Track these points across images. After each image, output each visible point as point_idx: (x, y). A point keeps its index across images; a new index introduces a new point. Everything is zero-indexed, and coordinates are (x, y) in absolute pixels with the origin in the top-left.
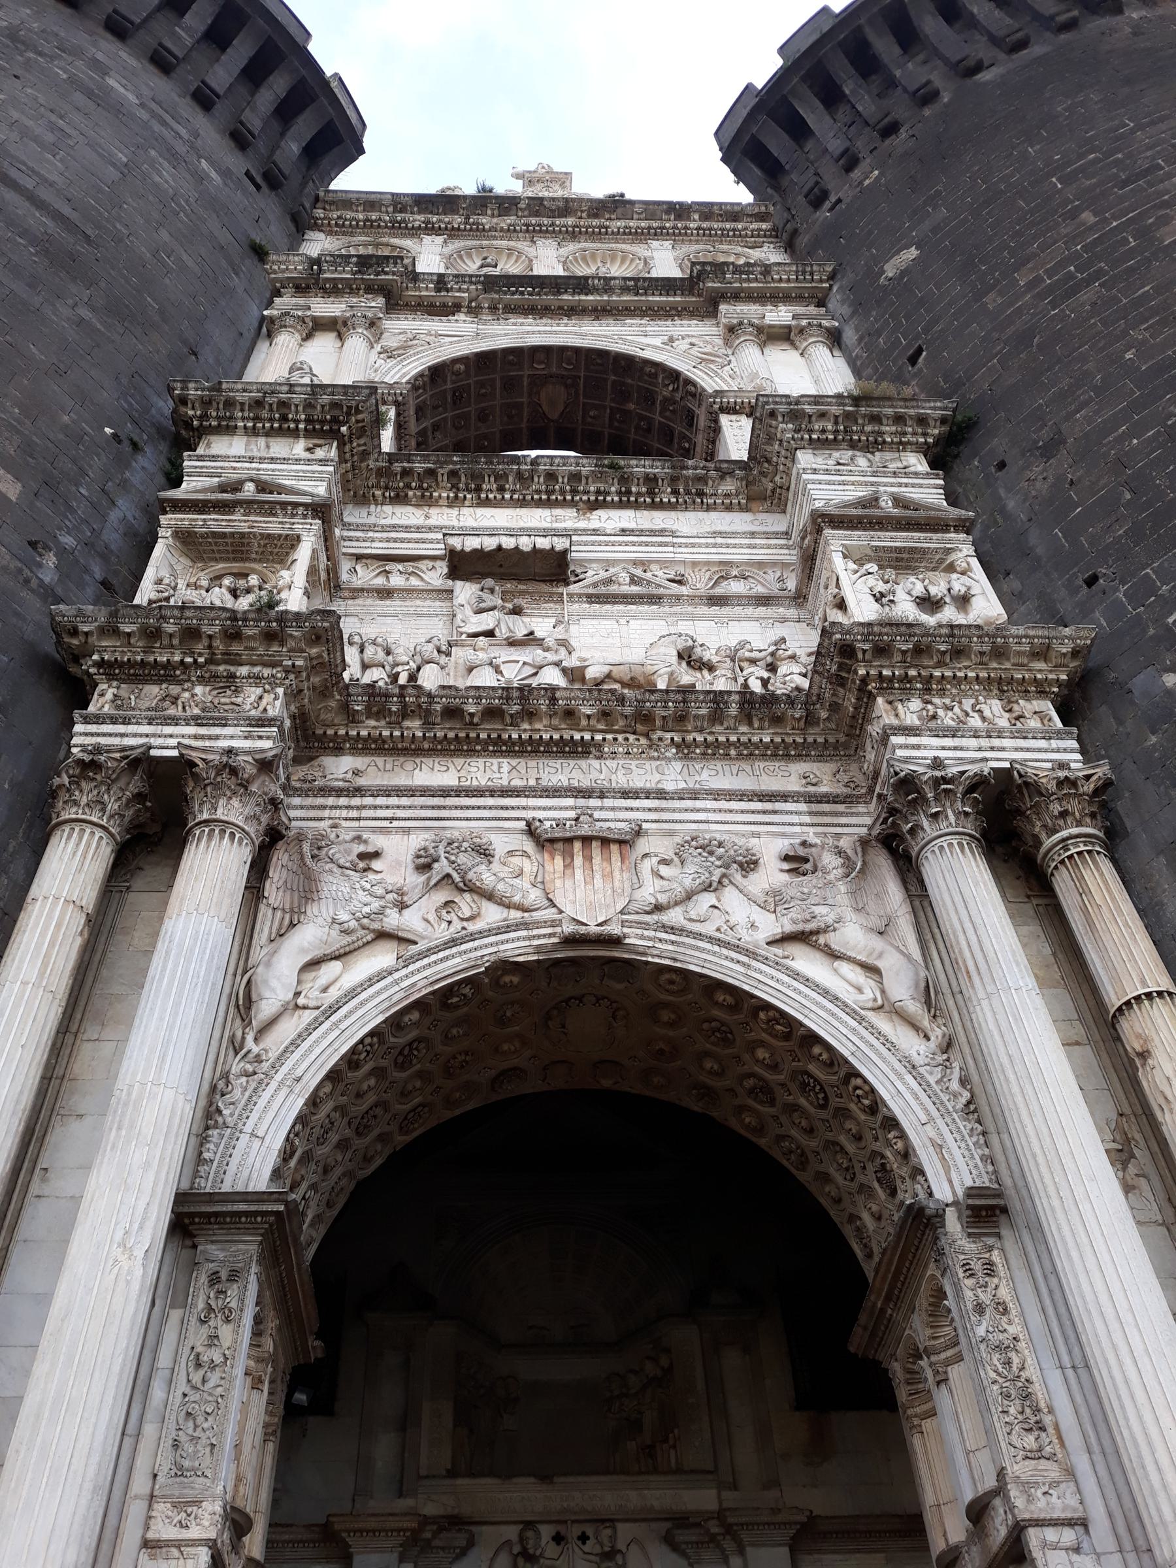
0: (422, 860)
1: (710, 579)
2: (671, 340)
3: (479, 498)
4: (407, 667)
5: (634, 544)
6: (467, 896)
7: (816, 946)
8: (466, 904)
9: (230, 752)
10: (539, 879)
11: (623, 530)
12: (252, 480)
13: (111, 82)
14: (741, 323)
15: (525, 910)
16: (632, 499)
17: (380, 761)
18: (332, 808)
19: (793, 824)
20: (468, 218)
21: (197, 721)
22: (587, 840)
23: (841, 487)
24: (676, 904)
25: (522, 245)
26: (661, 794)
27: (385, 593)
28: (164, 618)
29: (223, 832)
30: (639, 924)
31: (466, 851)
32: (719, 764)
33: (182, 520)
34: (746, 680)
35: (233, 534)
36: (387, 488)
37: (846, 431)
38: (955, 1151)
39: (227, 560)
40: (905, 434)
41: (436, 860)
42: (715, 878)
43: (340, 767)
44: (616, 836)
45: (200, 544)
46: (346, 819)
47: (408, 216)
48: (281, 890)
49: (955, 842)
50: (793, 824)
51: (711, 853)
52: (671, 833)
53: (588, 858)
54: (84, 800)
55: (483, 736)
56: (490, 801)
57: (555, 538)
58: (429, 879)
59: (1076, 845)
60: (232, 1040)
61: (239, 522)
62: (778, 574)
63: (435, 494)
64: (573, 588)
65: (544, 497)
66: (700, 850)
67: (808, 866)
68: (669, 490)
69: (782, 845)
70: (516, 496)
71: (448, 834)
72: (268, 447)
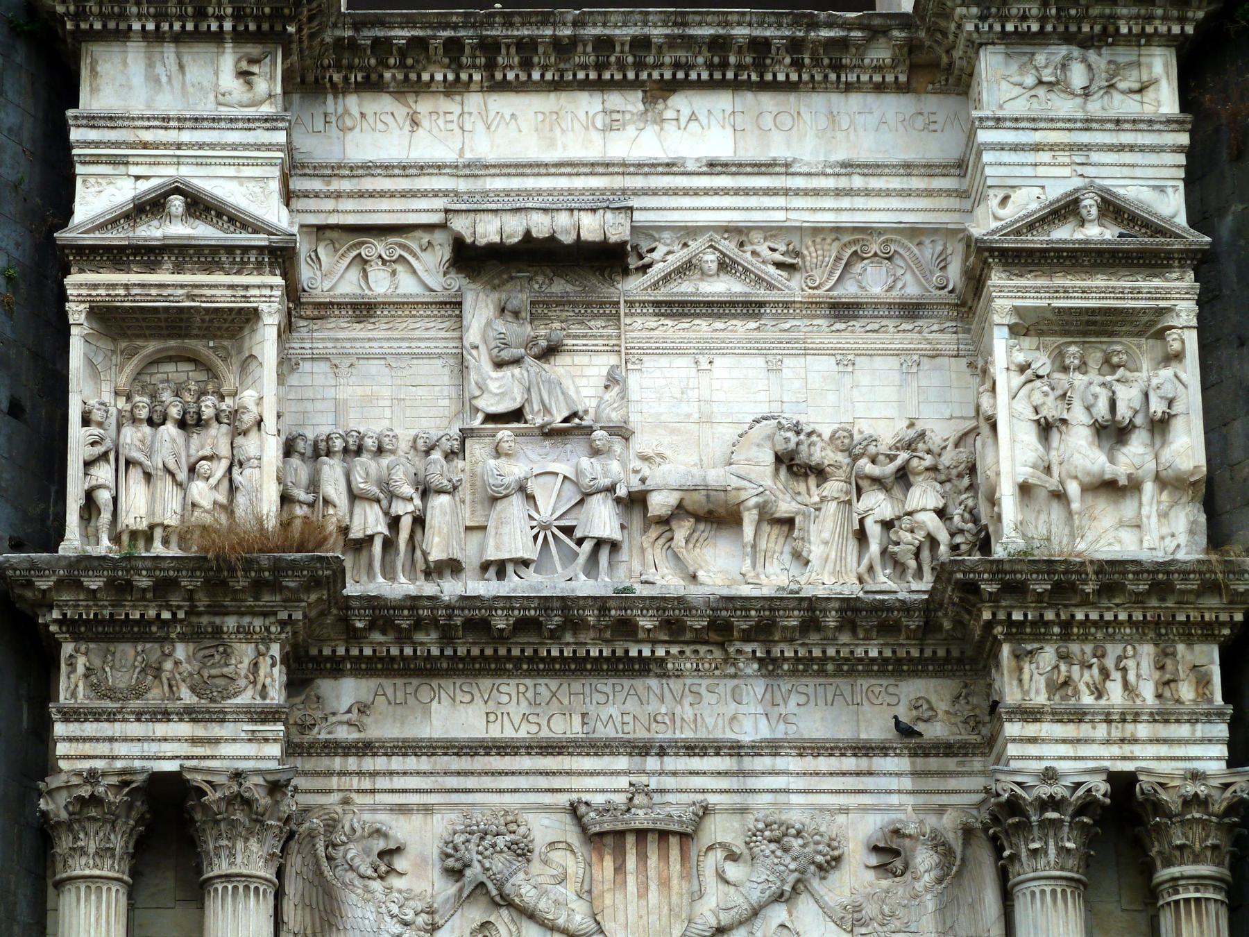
0: (450, 862)
1: (838, 259)
3: (493, 76)
4: (410, 508)
5: (726, 192)
6: (505, 913)
9: (238, 775)
10: (586, 887)
11: (711, 164)
12: (177, 191)
16: (730, 75)
17: (387, 684)
18: (342, 773)
19: (890, 792)
21: (190, 714)
22: (641, 834)
23: (1030, 157)
24: (741, 923)
26: (736, 749)
27: (363, 310)
28: (138, 571)
29: (247, 888)
31: (501, 852)
32: (811, 682)
33: (95, 286)
34: (861, 521)
35: (167, 309)
36: (351, 67)
37: (1058, 17)
39: (160, 337)
40: (1150, 18)
41: (467, 865)
42: (787, 888)
44: (676, 828)
45: (123, 320)
46: (358, 791)
48: (300, 907)
49: (1048, 889)
50: (890, 792)
51: (786, 850)
52: (743, 810)
53: (642, 857)
54: (92, 849)
55: (516, 652)
56: (526, 762)
57: (609, 215)
58: (461, 890)
59: (1186, 887)
62: (939, 248)
63: (426, 77)
64: (634, 286)
65: (593, 75)
66: (773, 846)
67: (898, 864)
68: (788, 60)
70: (549, 76)
71: (477, 816)
72: (181, 67)
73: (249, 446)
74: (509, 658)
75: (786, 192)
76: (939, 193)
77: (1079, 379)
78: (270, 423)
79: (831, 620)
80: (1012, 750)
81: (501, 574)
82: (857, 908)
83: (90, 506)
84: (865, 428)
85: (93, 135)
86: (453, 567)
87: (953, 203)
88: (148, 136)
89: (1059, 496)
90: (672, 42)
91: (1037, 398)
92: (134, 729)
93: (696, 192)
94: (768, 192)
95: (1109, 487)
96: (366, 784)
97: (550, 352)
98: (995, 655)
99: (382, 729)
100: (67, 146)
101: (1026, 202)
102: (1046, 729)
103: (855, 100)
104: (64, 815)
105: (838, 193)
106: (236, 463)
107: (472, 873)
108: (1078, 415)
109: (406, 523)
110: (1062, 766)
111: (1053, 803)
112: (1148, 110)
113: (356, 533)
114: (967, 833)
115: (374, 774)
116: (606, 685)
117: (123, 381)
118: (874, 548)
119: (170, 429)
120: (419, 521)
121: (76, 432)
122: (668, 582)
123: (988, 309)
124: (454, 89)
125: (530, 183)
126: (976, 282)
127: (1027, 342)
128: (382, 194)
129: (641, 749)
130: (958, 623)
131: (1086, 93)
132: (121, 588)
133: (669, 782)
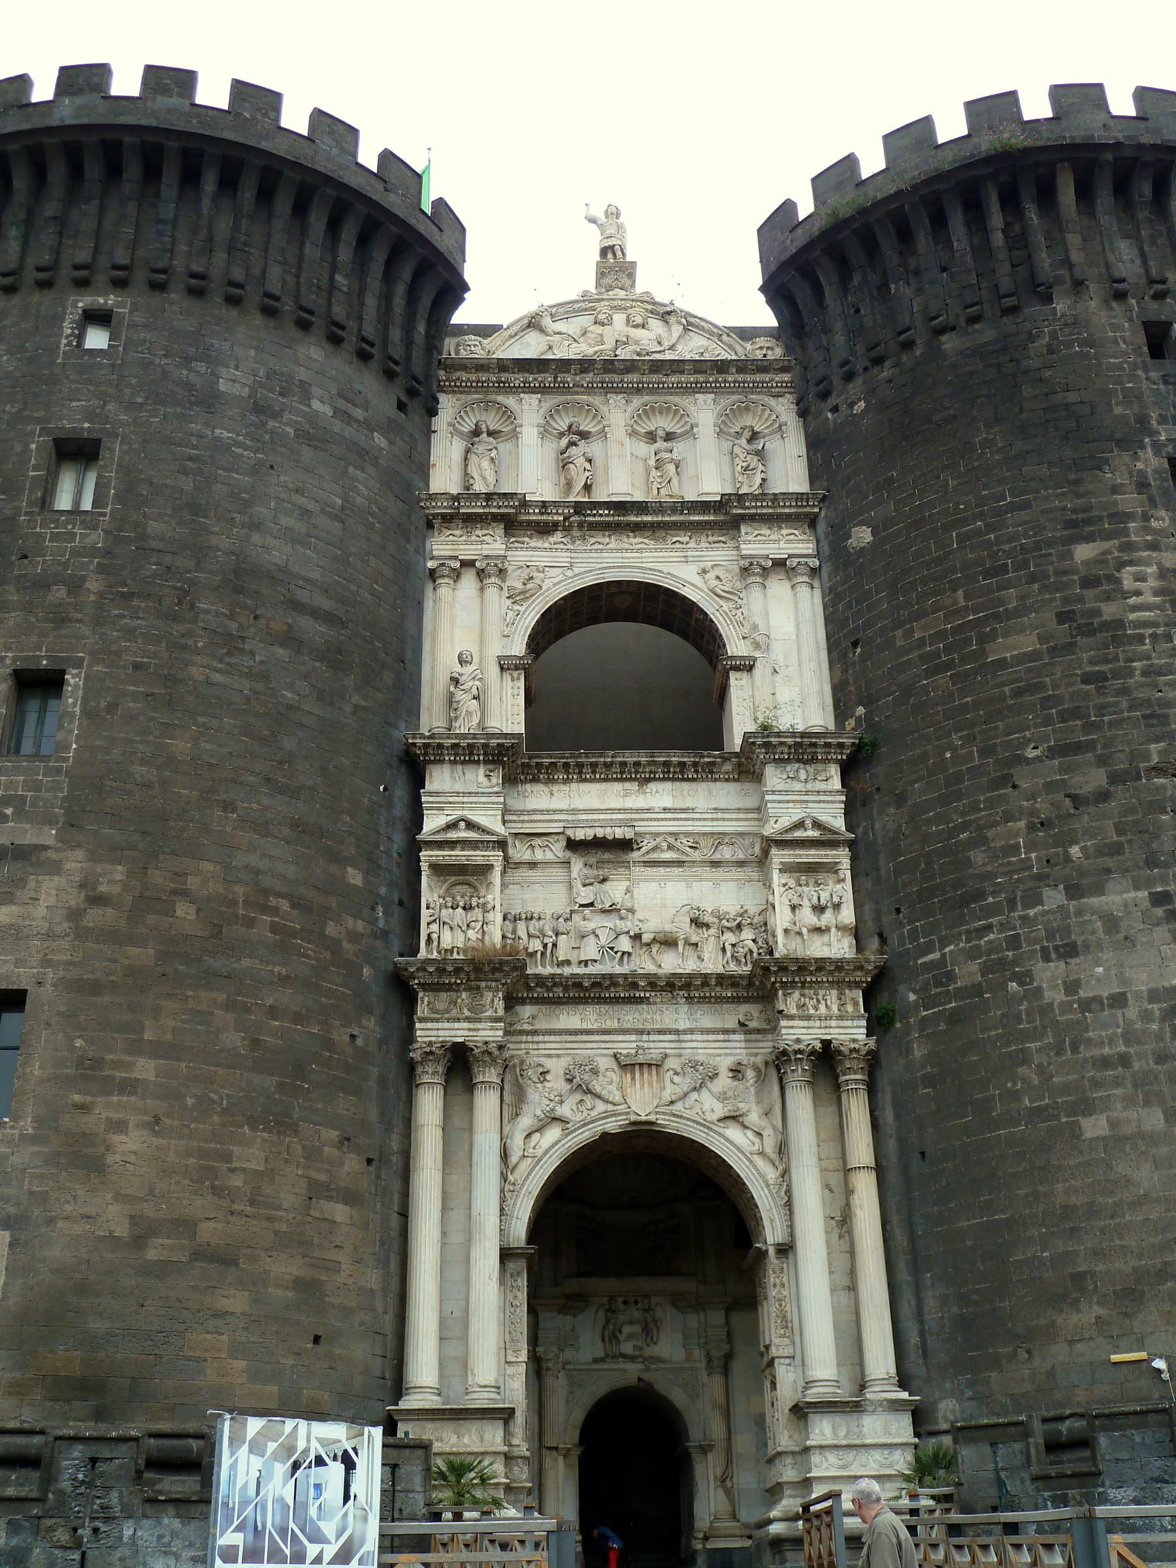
2: (704, 571)
5: (670, 819)
7: (738, 1122)
8: (588, 1099)
9: (486, 1043)
13: (316, 405)
14: (751, 564)
15: (615, 1104)
17: (543, 1008)
20: (555, 378)
21: (468, 1019)
22: (641, 1065)
23: (786, 805)
25: (597, 400)
26: (677, 1032)
27: (533, 865)
30: (663, 1113)
38: (778, 1223)
40: (829, 753)
43: (527, 1011)
47: (512, 377)
52: (680, 1056)
53: (642, 1074)
56: (597, 1038)
60: (502, 1173)
61: (459, 855)
64: (635, 855)
67: (740, 1076)
69: (729, 1061)
71: (578, 1058)
73: (490, 916)
74: (590, 997)
75: (693, 819)
76: (751, 819)
77: (805, 888)
78: (498, 908)
79: (713, 982)
80: (784, 1031)
81: (586, 965)
82: (725, 1093)
83: (429, 939)
84: (724, 909)
85: (431, 799)
86: (568, 962)
87: (756, 823)
88: (451, 799)
89: (799, 934)
90: (649, 763)
91: (790, 896)
92: (446, 1025)
93: (659, 820)
94: (686, 819)
95: (818, 930)
96: (535, 1046)
97: (604, 880)
98: (776, 994)
99: (541, 1025)
100: (421, 803)
101: (785, 822)
102: (796, 1023)
103: (718, 784)
104: (419, 1059)
105: (713, 819)
106: (485, 923)
107: (577, 1080)
108: (806, 903)
109: (550, 946)
110: (802, 1037)
111: (800, 1051)
112: (830, 788)
113: (530, 950)
114: (767, 1063)
115: (538, 1042)
116: (627, 1007)
117: (442, 892)
118: (729, 954)
119: (460, 910)
120: (555, 945)
121: (424, 911)
122: (650, 968)
123: (771, 863)
124: (566, 781)
125: (596, 817)
126: (766, 853)
127: (786, 875)
128: (540, 821)
129: (641, 1032)
130: (762, 983)
131: (806, 781)
132: (441, 971)
133: (652, 1045)
